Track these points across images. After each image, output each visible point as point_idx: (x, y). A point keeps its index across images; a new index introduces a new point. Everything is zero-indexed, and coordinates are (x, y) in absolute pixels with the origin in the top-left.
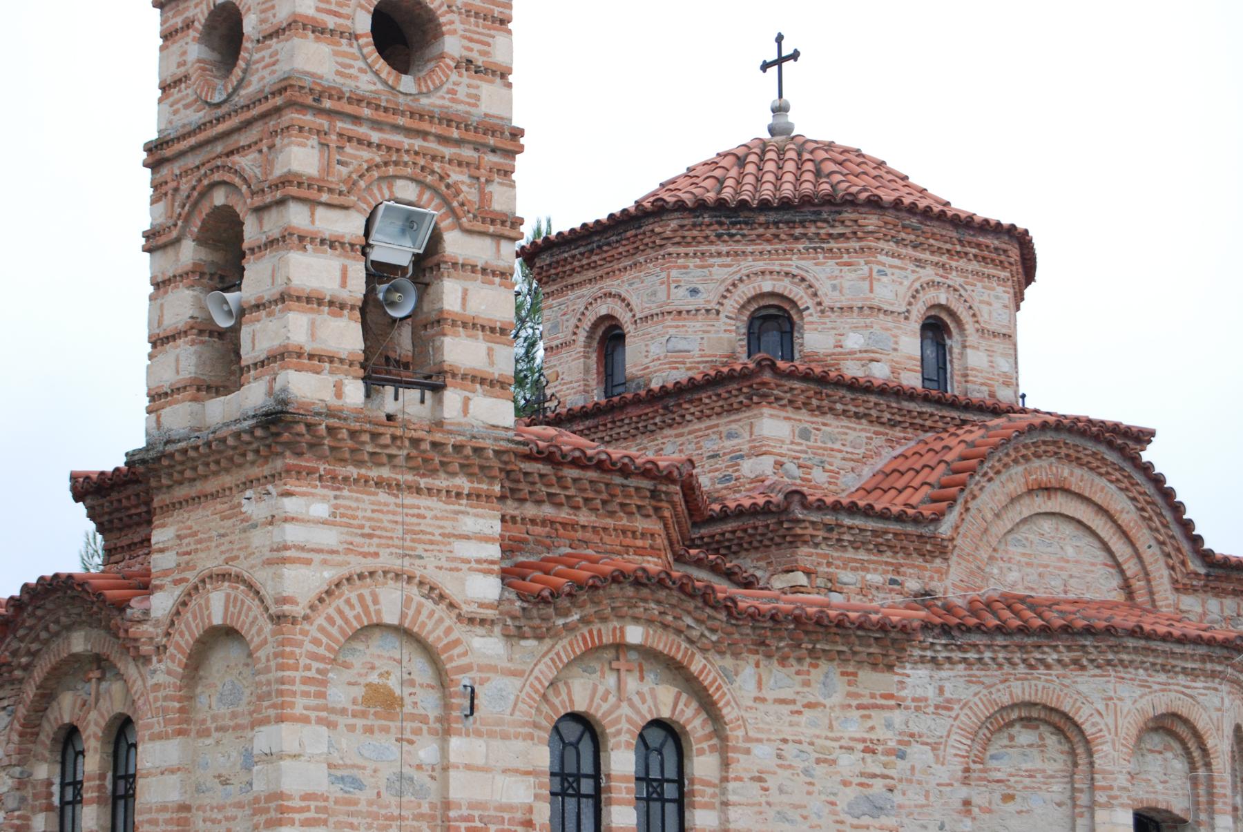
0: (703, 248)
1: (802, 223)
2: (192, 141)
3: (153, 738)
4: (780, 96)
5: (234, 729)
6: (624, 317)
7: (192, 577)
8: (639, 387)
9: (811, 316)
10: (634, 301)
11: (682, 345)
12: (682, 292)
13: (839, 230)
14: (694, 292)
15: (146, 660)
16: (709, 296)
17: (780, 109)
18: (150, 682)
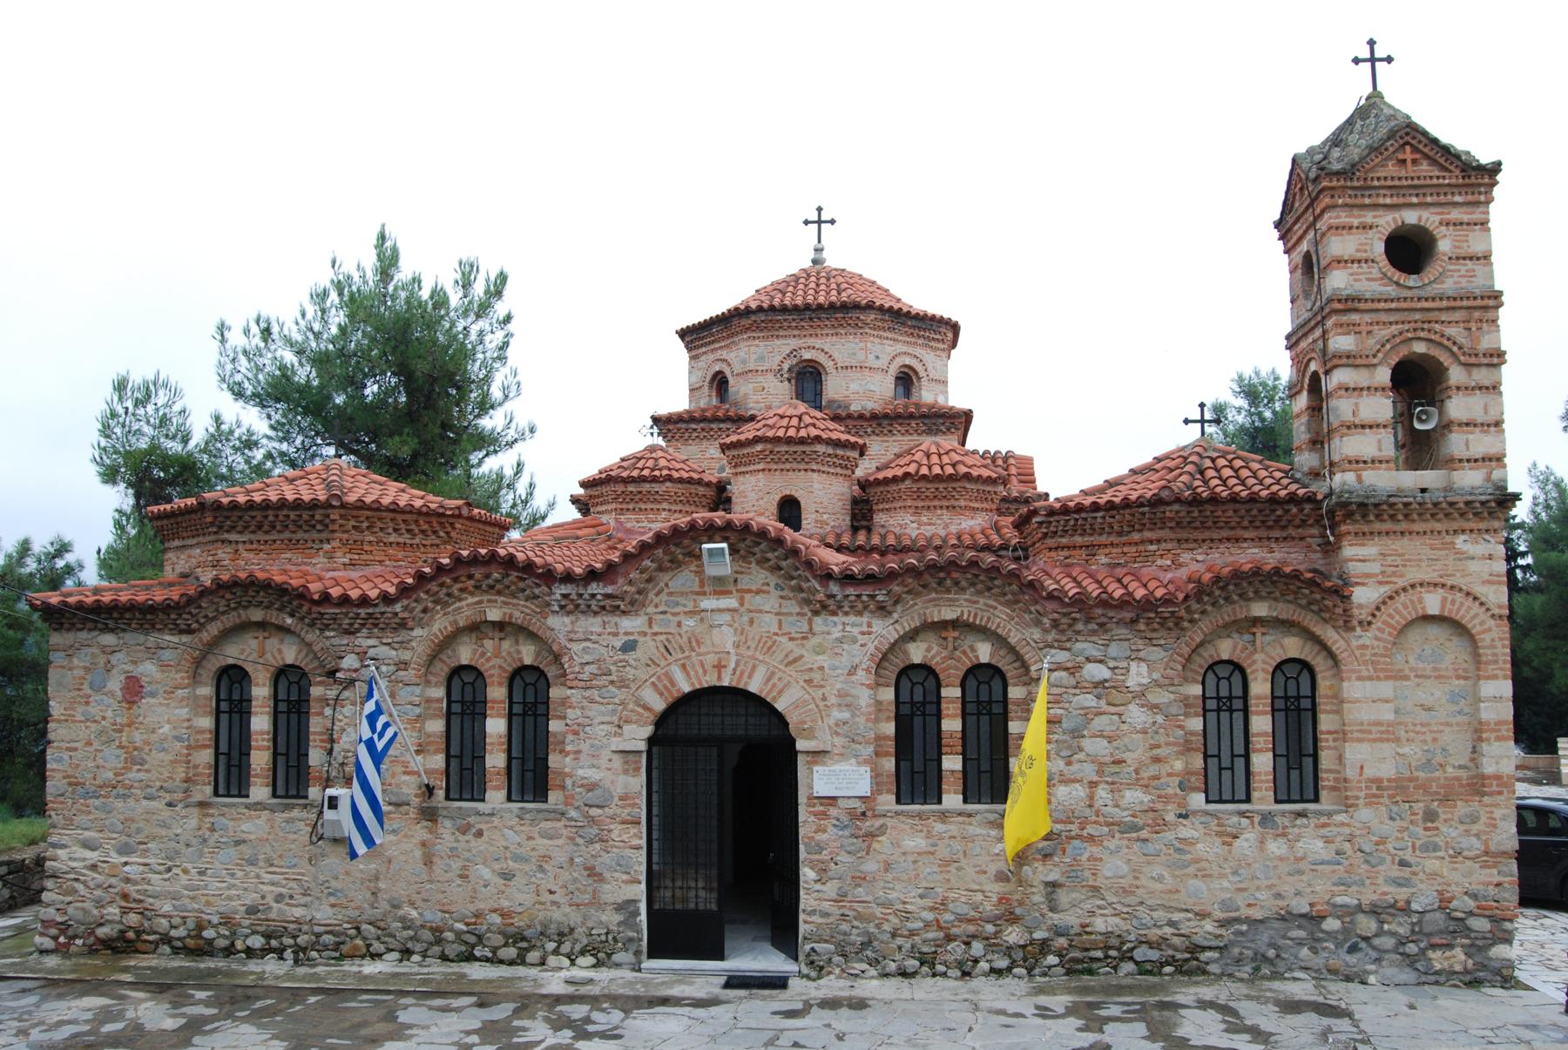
0: (881, 333)
1: (924, 330)
2: (1393, 305)
3: (1360, 678)
4: (819, 241)
5: (1436, 677)
6: (828, 364)
7: (1401, 583)
8: (840, 407)
9: (924, 381)
10: (836, 355)
11: (872, 388)
12: (871, 357)
13: (937, 337)
14: (877, 357)
15: (1353, 629)
16: (883, 363)
17: (818, 250)
18: (1354, 643)
